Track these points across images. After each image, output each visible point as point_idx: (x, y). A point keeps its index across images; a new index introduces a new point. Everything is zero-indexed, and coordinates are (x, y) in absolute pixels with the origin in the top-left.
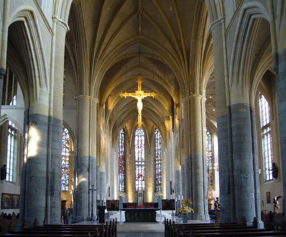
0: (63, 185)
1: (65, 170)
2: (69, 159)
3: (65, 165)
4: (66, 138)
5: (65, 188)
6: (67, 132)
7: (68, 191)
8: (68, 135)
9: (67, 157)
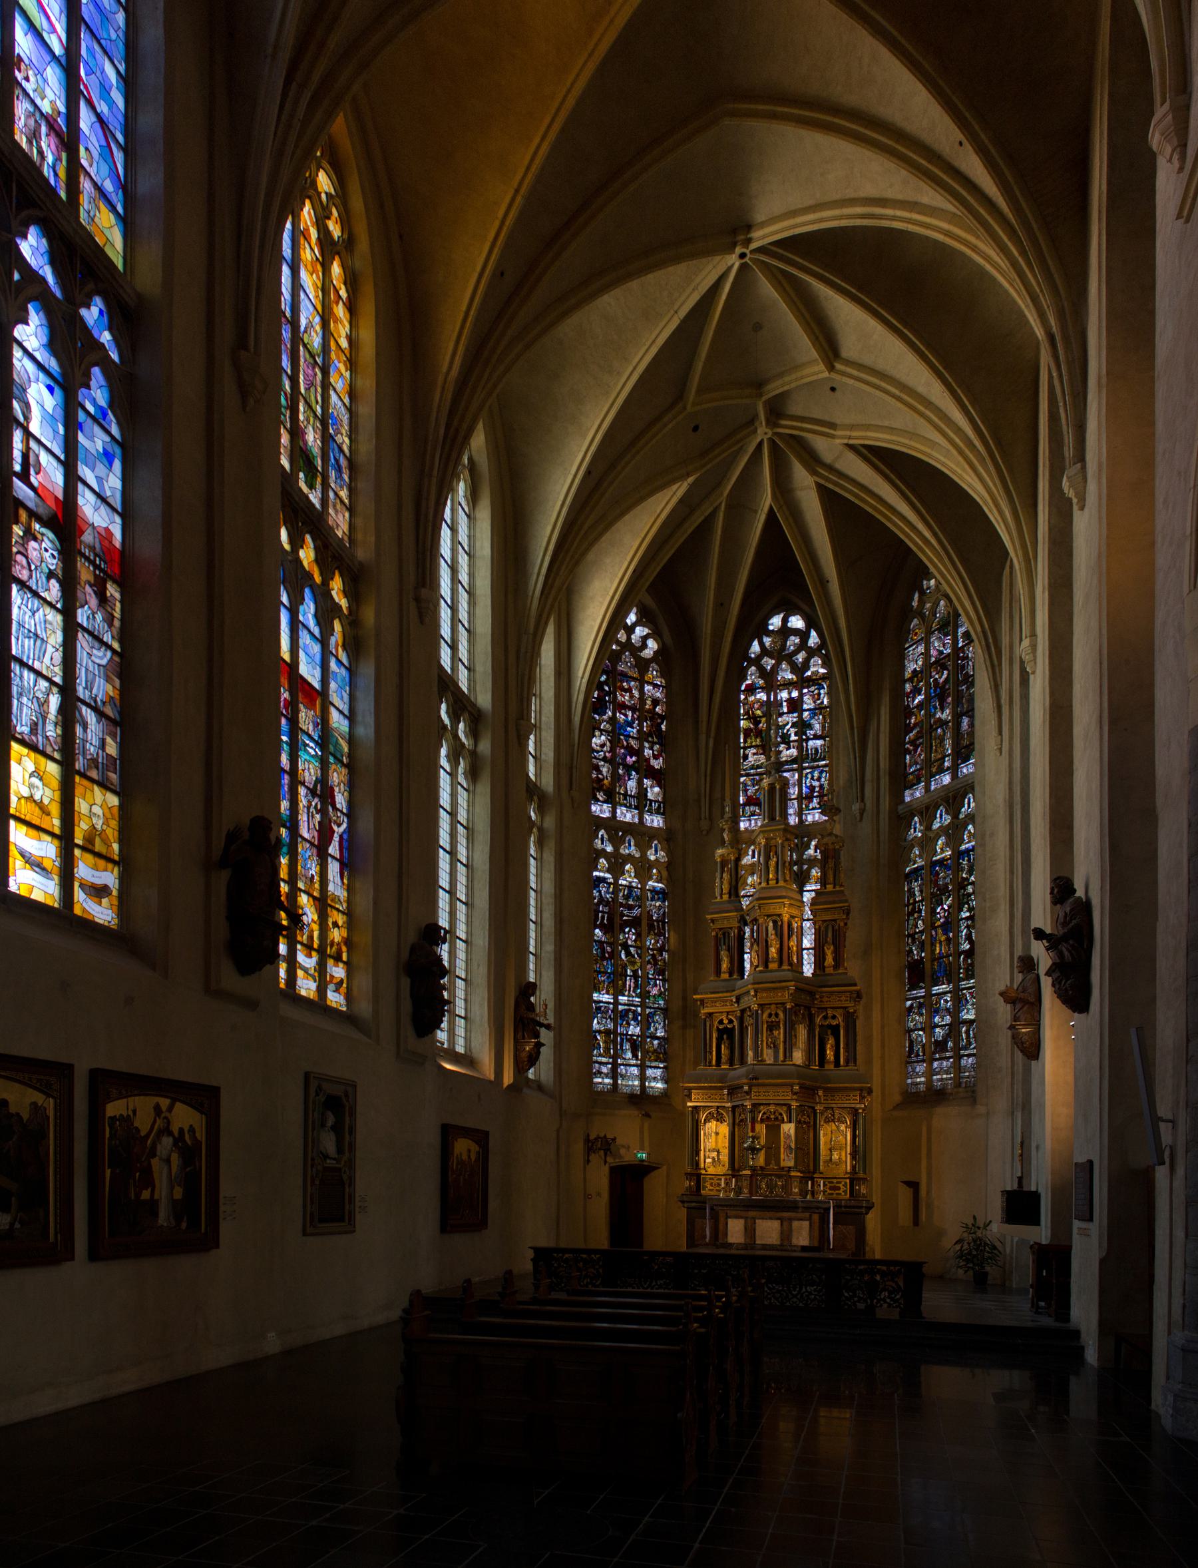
0: (629, 1055)
1: (638, 935)
2: (670, 853)
3: (641, 899)
4: (642, 699)
5: (643, 1078)
6: (648, 653)
7: (665, 1094)
8: (653, 673)
9: (652, 838)
